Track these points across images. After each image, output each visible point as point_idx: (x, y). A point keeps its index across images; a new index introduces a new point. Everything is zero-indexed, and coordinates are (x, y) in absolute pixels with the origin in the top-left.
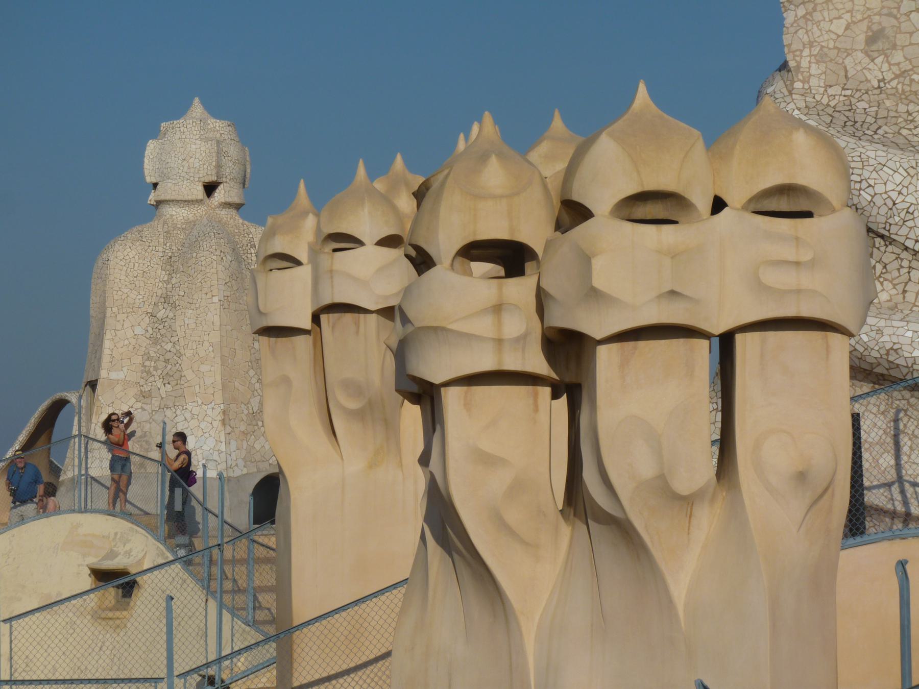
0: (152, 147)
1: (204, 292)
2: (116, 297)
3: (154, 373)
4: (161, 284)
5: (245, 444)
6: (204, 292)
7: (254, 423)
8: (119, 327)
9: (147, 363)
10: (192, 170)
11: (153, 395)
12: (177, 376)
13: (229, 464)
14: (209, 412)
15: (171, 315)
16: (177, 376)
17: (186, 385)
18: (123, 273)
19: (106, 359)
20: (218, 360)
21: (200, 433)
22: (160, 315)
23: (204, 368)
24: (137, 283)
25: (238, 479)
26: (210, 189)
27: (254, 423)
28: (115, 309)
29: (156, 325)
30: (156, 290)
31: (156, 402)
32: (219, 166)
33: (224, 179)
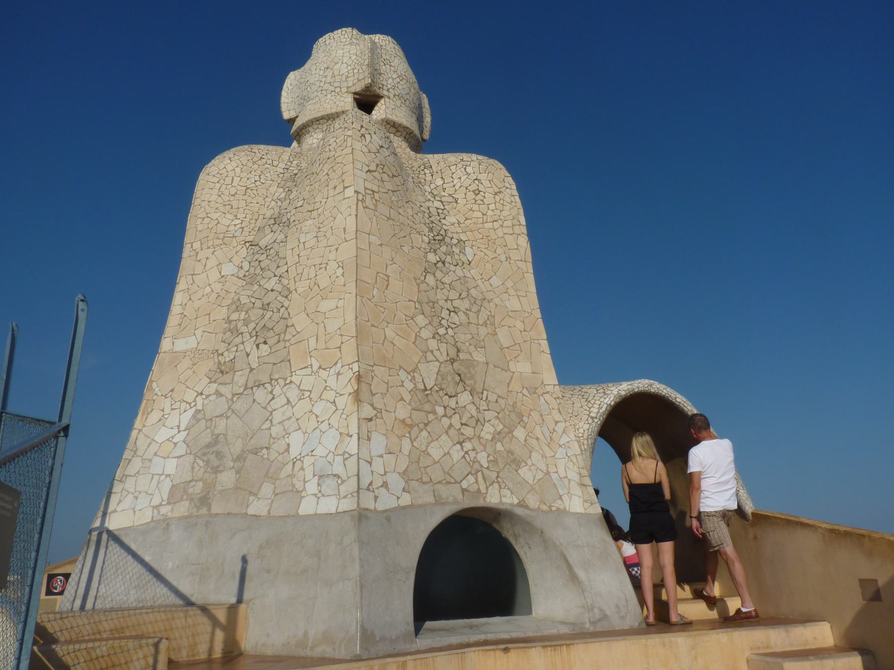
0: (292, 78)
1: (331, 186)
2: (200, 228)
3: (244, 329)
4: (273, 203)
5: (406, 445)
6: (331, 186)
7: (427, 407)
8: (199, 268)
9: (234, 316)
10: (338, 78)
11: (238, 366)
12: (279, 328)
13: (365, 482)
14: (332, 382)
15: (281, 237)
16: (279, 328)
17: (293, 341)
18: (215, 191)
19: (173, 320)
20: (352, 287)
21: (313, 423)
22: (263, 243)
23: (326, 305)
24: (235, 204)
25: (388, 515)
26: (366, 102)
27: (427, 407)
28: (197, 245)
29: (257, 256)
30: (264, 210)
31: (240, 379)
32: (375, 72)
33: (385, 93)
